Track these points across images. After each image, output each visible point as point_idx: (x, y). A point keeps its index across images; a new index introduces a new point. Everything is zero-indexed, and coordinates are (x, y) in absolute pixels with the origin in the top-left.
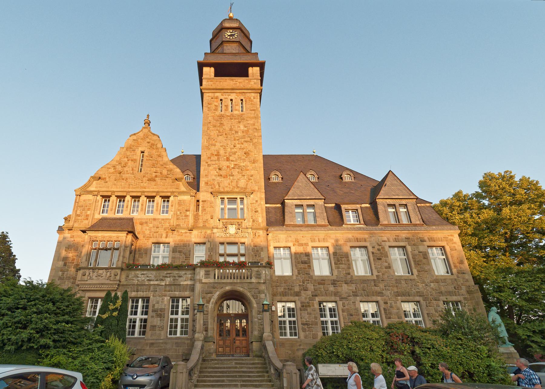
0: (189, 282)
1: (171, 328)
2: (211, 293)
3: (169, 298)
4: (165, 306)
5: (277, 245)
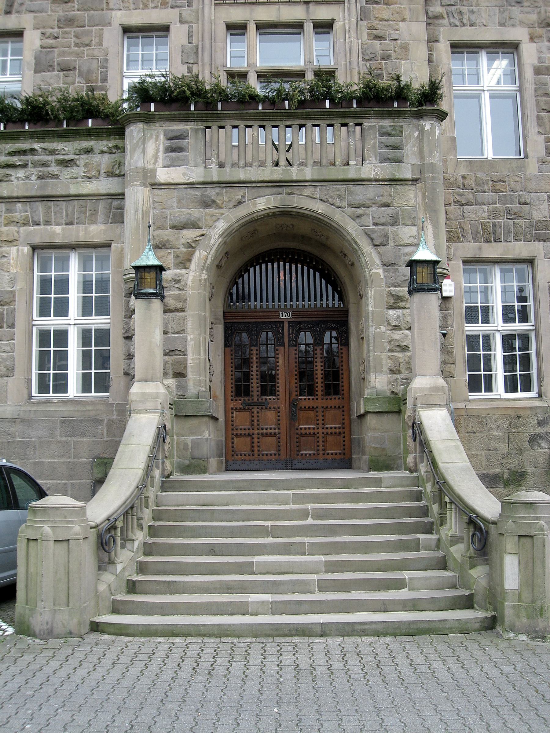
0: (104, 185)
1: (43, 357)
2: (194, 225)
3: (26, 249)
4: (13, 281)
5: (466, 34)
